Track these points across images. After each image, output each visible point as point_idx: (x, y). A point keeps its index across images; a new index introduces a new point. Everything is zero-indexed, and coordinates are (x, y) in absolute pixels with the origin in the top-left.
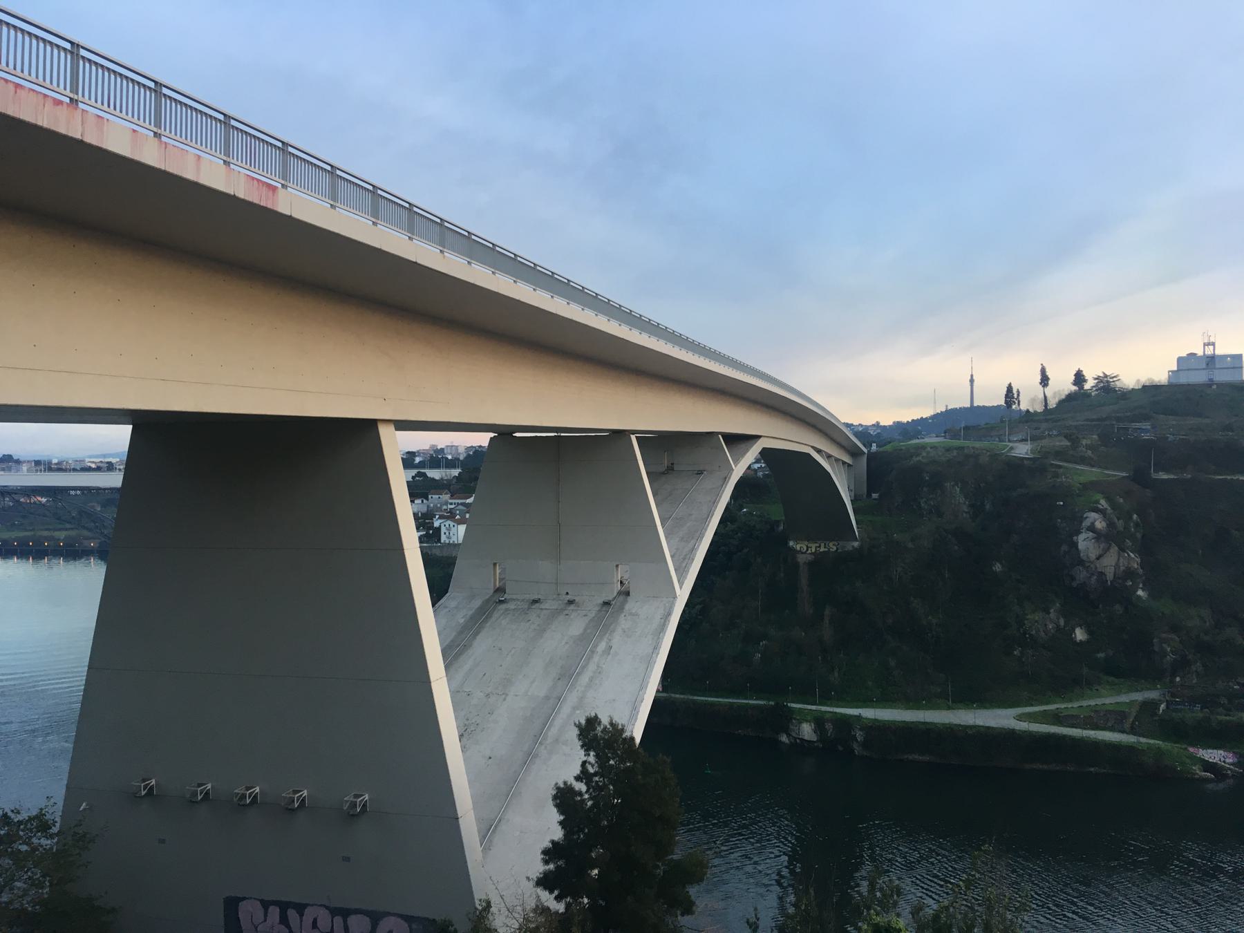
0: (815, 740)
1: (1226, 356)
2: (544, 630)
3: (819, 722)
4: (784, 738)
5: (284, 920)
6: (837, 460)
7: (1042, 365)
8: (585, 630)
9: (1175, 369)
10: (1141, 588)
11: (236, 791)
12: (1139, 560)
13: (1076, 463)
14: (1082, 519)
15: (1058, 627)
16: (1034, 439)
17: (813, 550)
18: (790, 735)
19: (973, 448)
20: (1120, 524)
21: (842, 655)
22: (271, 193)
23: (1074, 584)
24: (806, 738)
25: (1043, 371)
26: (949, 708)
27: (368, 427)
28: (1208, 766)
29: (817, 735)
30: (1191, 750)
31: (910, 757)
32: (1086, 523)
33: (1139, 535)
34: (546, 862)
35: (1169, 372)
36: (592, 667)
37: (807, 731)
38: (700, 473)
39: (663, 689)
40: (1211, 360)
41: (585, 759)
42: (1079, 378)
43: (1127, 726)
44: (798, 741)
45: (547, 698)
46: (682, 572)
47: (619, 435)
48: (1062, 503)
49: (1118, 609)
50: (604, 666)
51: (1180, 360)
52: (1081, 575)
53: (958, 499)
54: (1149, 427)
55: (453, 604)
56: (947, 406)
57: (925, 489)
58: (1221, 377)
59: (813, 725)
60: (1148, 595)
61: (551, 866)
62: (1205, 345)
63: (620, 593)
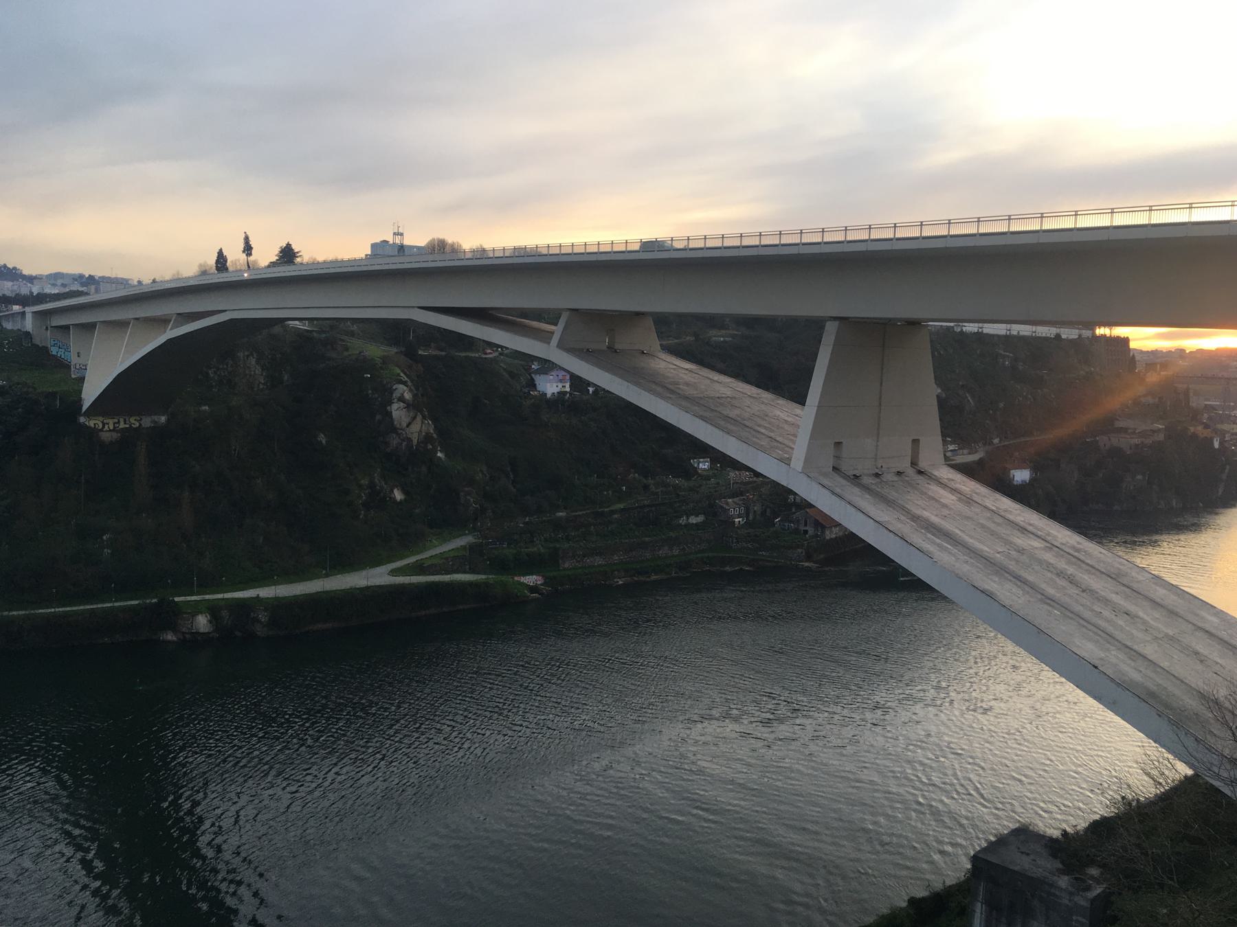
1: (412, 247)
4: (170, 636)
7: (245, 233)
9: (370, 253)
14: (391, 391)
17: (112, 428)
23: (388, 450)
24: (202, 630)
25: (247, 239)
26: (327, 576)
30: (516, 578)
32: (396, 395)
37: (202, 622)
49: (424, 469)
52: (394, 441)
53: (253, 369)
62: (394, 234)
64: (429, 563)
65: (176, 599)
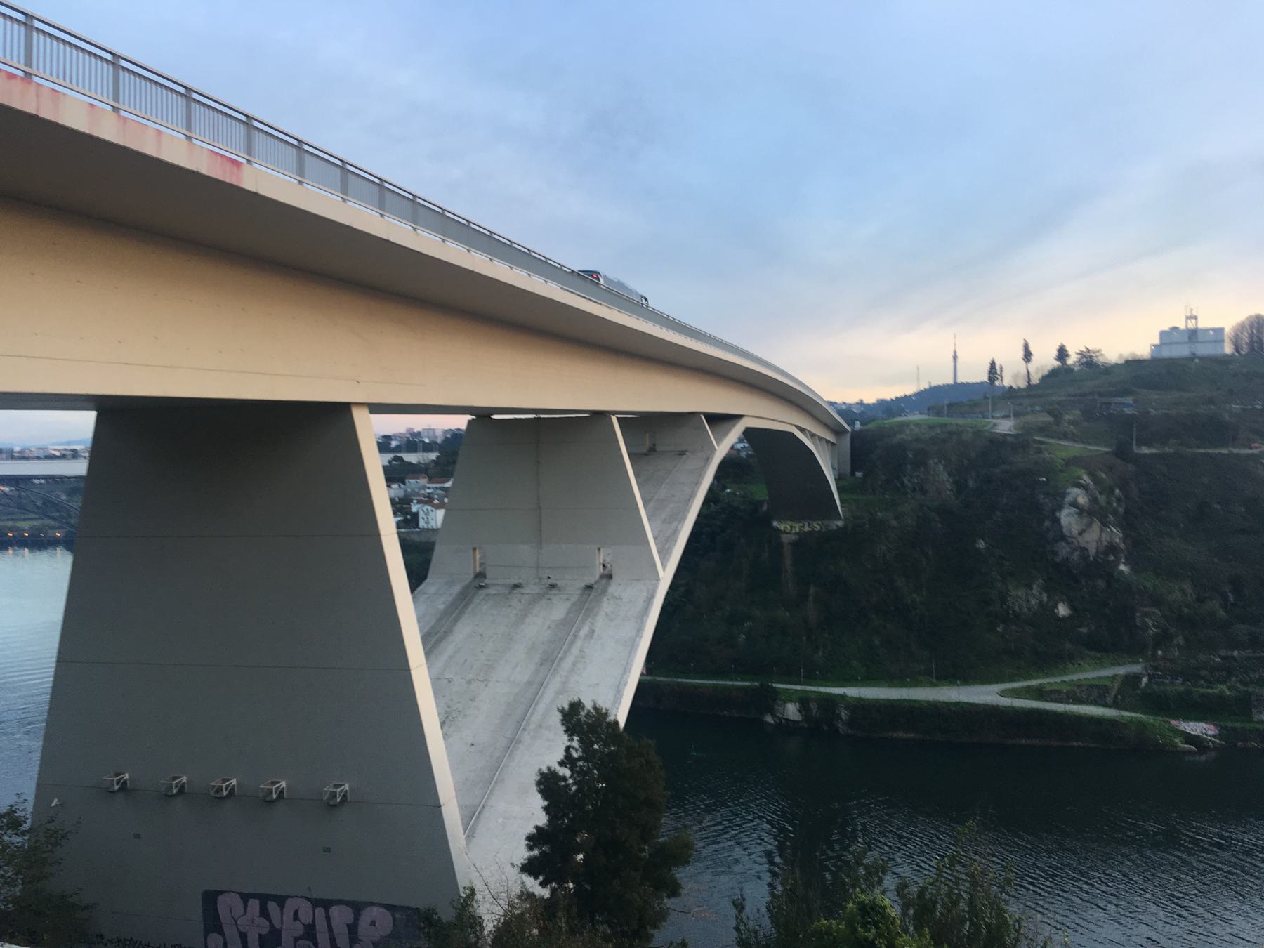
0: (800, 719)
1: (1207, 330)
2: (526, 615)
3: (804, 701)
4: (769, 719)
5: (264, 913)
6: (821, 439)
8: (568, 613)
10: (1123, 563)
11: (213, 784)
12: (1121, 535)
13: (1060, 439)
14: (1064, 495)
15: (1041, 602)
16: (1017, 415)
17: (797, 530)
18: (775, 715)
19: (957, 425)
20: (1102, 499)
21: (826, 635)
22: (235, 169)
23: (1058, 560)
24: (791, 718)
26: (934, 685)
27: (340, 412)
28: (1189, 738)
29: (802, 715)
30: (1173, 722)
31: (895, 735)
32: (1069, 499)
33: (1121, 510)
34: (531, 848)
35: (1151, 345)
36: (575, 651)
37: (792, 711)
38: (682, 453)
39: (647, 671)
40: (1193, 334)
41: (568, 744)
42: (1062, 353)
43: (1109, 700)
44: (783, 721)
45: (529, 683)
46: (665, 553)
47: (600, 416)
48: (1044, 479)
49: (1101, 584)
50: (587, 650)
51: (1163, 334)
52: (1063, 550)
53: (941, 476)
54: (1131, 402)
55: (432, 589)
56: (930, 383)
57: (909, 467)
58: (1204, 350)
59: (798, 705)
60: (1131, 570)
61: (536, 852)
62: (1188, 318)
63: (602, 577)
64: (1048, 688)
65: (774, 685)
